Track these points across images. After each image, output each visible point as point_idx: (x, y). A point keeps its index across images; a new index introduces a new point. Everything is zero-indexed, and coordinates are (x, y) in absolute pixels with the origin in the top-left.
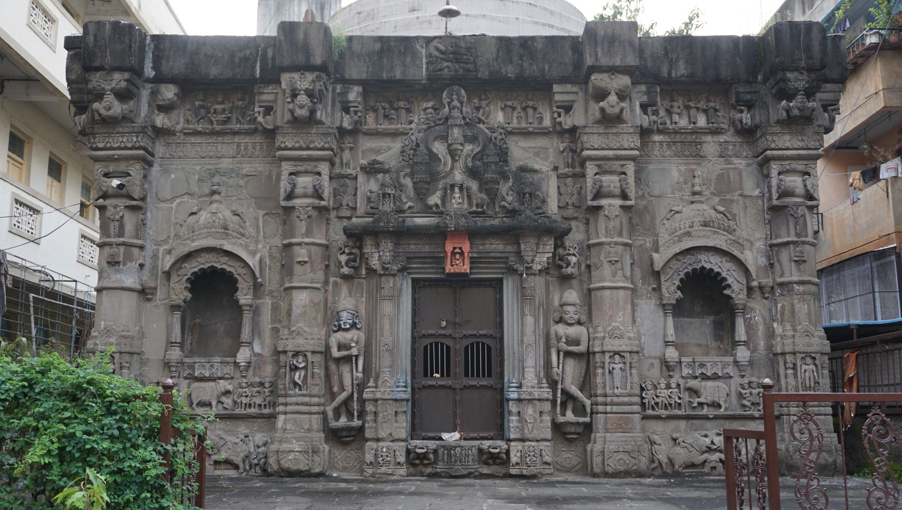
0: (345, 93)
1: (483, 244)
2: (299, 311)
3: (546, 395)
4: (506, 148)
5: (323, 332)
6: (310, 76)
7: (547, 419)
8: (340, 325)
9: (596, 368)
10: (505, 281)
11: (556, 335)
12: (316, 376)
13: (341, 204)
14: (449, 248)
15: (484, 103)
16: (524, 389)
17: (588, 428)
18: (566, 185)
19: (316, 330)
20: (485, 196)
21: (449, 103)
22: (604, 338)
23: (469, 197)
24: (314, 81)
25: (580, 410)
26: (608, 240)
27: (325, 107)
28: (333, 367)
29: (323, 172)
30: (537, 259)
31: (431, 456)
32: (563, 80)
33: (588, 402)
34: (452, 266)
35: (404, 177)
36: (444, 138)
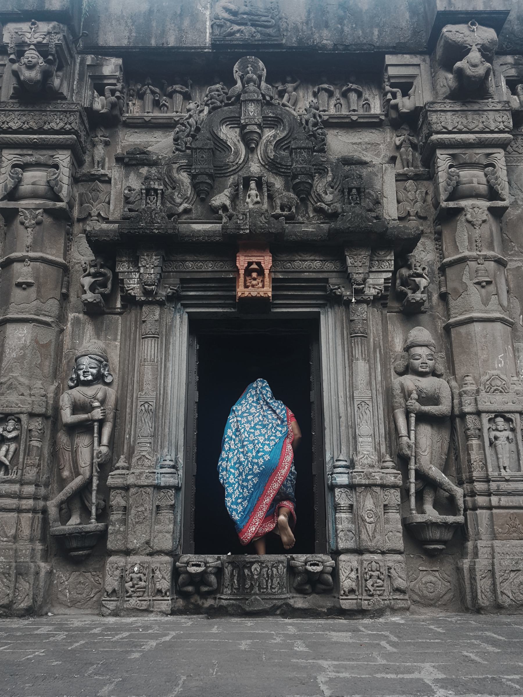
0: (97, 66)
1: (290, 261)
2: (14, 355)
3: (391, 479)
4: (322, 134)
5: (53, 388)
6: (44, 27)
7: (395, 516)
8: (78, 376)
9: (467, 438)
10: (322, 317)
11: (403, 390)
12: (34, 452)
13: (90, 215)
14: (242, 262)
15: (290, 87)
16: (358, 468)
17: (460, 533)
18: (405, 189)
19: (39, 384)
20: (292, 195)
21: (242, 78)
22: (478, 391)
23: (271, 198)
24: (49, 33)
25: (448, 505)
26: (474, 254)
27: (69, 78)
28: (63, 438)
29: (61, 164)
30: (370, 281)
31: (213, 579)
32: (398, 49)
33: (459, 492)
34: (246, 287)
35: (179, 170)
36: (234, 121)
